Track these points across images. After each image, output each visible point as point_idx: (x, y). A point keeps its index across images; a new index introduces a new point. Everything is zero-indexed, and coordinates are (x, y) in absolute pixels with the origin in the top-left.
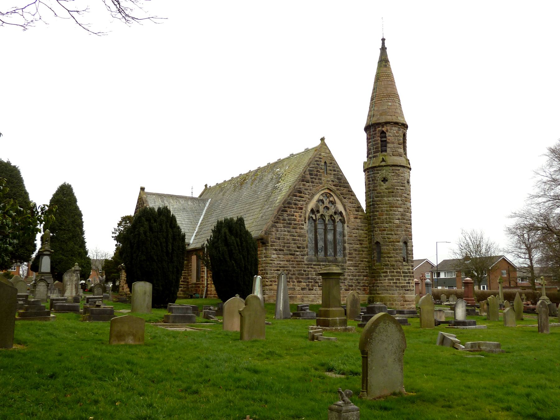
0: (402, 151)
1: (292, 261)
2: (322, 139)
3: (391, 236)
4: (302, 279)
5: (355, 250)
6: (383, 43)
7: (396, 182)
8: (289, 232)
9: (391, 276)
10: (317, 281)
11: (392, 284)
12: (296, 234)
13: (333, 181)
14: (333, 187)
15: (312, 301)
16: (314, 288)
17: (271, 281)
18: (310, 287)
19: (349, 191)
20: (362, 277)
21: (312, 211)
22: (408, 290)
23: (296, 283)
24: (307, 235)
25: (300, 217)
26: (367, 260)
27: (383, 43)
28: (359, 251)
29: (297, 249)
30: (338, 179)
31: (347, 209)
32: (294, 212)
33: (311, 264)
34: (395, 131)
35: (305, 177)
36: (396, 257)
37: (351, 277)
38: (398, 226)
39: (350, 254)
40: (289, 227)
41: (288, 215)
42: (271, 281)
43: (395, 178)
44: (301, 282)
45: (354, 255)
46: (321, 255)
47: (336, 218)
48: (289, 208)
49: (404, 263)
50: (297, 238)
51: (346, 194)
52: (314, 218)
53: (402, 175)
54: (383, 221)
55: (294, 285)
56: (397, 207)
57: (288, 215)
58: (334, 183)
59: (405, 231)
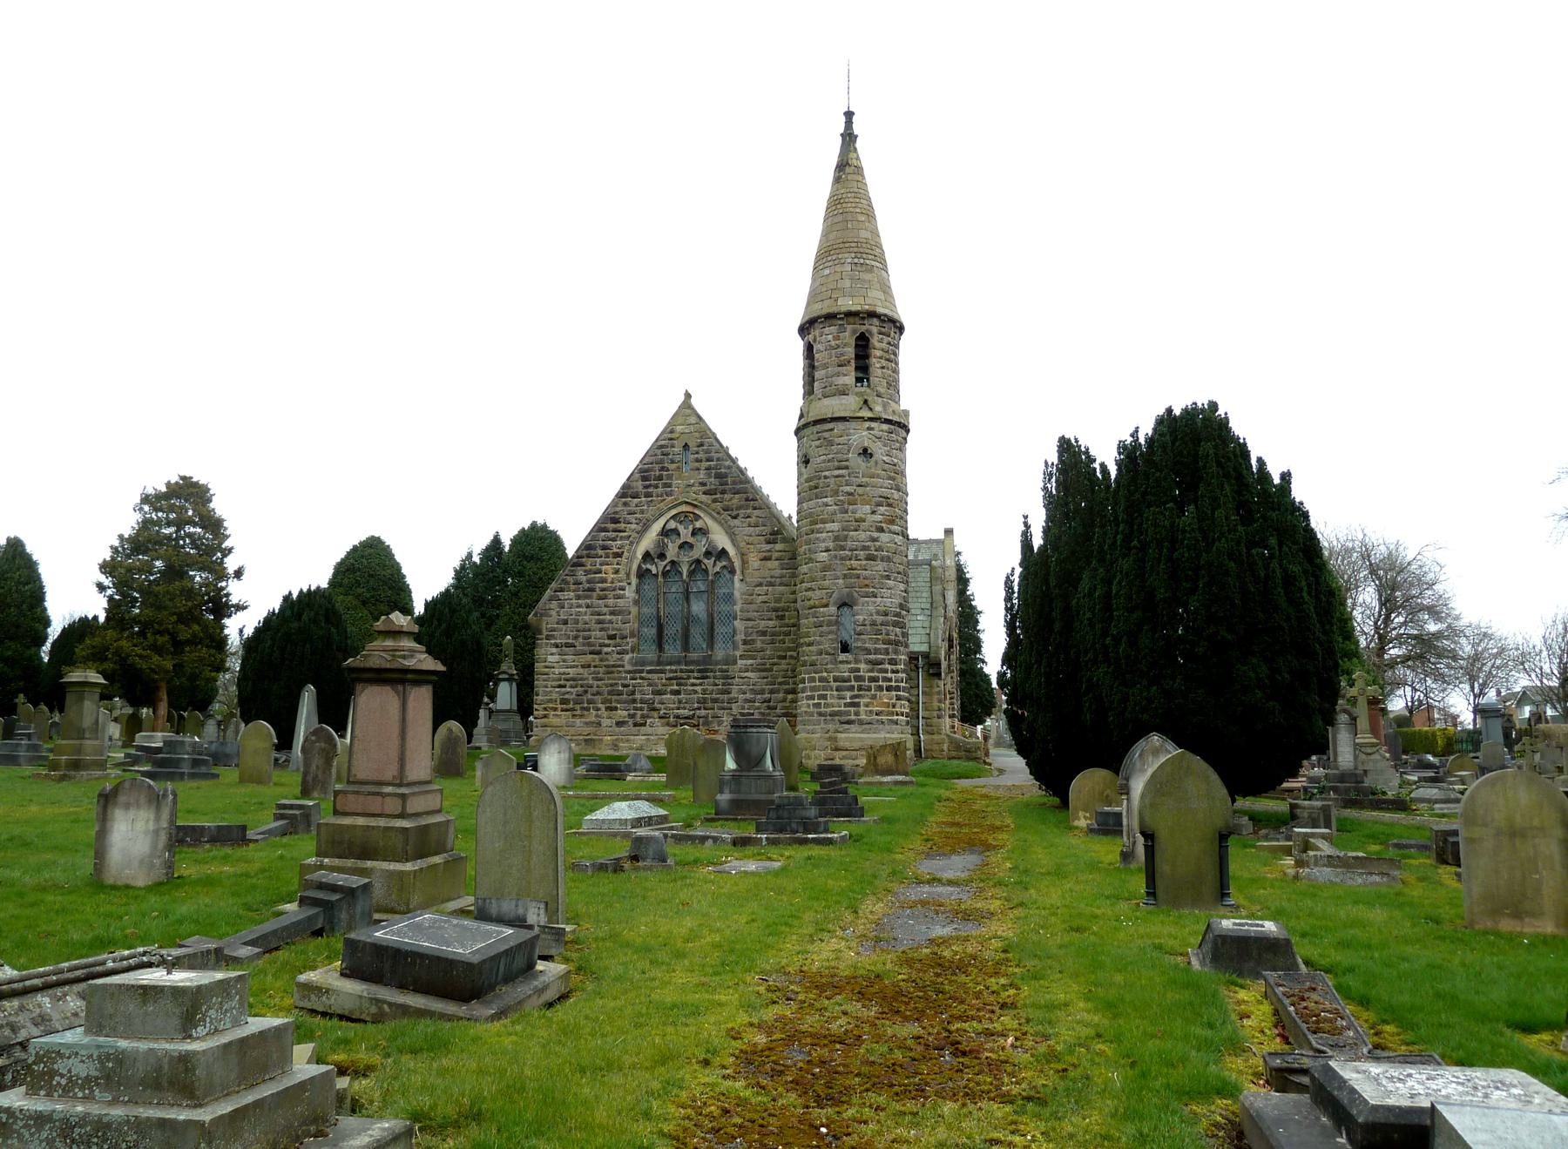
0: (849, 378)
2: (688, 396)
5: (764, 633)
14: (704, 498)
18: (638, 719)
20: (781, 695)
21: (647, 556)
22: (849, 722)
23: (603, 713)
28: (773, 634)
30: (718, 476)
36: (819, 643)
37: (748, 696)
39: (745, 642)
40: (587, 597)
41: (587, 572)
43: (822, 451)
45: (759, 645)
46: (673, 650)
47: (709, 569)
48: (588, 556)
49: (842, 657)
51: (739, 508)
56: (824, 522)
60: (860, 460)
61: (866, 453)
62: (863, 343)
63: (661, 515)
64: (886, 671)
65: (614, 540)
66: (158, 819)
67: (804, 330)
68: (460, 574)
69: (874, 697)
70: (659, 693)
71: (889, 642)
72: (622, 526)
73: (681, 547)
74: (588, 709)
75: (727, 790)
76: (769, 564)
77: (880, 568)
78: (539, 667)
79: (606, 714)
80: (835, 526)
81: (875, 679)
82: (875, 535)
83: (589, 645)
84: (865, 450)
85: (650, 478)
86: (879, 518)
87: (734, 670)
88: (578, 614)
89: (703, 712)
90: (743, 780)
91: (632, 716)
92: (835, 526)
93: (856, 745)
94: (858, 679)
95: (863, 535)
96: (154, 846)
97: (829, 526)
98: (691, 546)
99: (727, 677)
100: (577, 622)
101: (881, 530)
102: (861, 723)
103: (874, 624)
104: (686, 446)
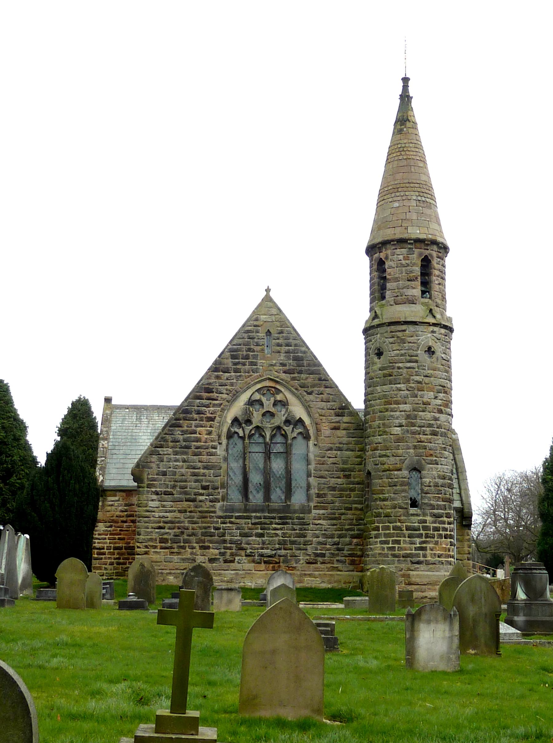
0: (417, 292)
1: (190, 512)
2: (268, 290)
3: (384, 459)
5: (333, 489)
6: (405, 87)
7: (397, 355)
8: (184, 461)
9: (386, 535)
11: (386, 551)
13: (283, 365)
14: (283, 376)
15: (230, 581)
16: (237, 558)
17: (146, 547)
18: (228, 557)
19: (320, 379)
20: (348, 539)
21: (236, 421)
22: (419, 563)
23: (198, 551)
24: (224, 466)
25: (210, 433)
26: (359, 506)
27: (405, 87)
29: (201, 491)
30: (296, 359)
32: (196, 427)
33: (231, 517)
34: (401, 257)
35: (220, 363)
36: (393, 499)
37: (321, 539)
39: (318, 496)
40: (186, 453)
42: (146, 547)
43: (395, 347)
44: (208, 548)
45: (329, 498)
48: (185, 419)
49: (412, 510)
50: (202, 471)
51: (313, 386)
52: (241, 434)
53: (410, 339)
54: (375, 432)
55: (192, 553)
56: (397, 403)
57: (184, 432)
58: (287, 368)
59: (415, 447)
60: (426, 356)
61: (430, 351)
62: (426, 263)
63: (248, 388)
64: (444, 523)
65: (207, 406)
66: (451, 630)
68: (22, 422)
69: (436, 543)
72: (215, 395)
73: (264, 415)
74: (184, 548)
75: (521, 614)
77: (440, 442)
79: (199, 552)
80: (407, 407)
81: (436, 529)
82: (437, 415)
83: (186, 493)
84: (430, 348)
85: (238, 357)
86: (439, 402)
87: (309, 518)
88: (175, 467)
89: (283, 552)
90: (533, 607)
92: (407, 407)
93: (425, 581)
94: (426, 528)
95: (428, 415)
96: (450, 647)
97: (402, 407)
98: (272, 415)
99: (304, 524)
100: (174, 474)
101: (440, 411)
102: (428, 563)
103: (436, 485)
104: (269, 333)
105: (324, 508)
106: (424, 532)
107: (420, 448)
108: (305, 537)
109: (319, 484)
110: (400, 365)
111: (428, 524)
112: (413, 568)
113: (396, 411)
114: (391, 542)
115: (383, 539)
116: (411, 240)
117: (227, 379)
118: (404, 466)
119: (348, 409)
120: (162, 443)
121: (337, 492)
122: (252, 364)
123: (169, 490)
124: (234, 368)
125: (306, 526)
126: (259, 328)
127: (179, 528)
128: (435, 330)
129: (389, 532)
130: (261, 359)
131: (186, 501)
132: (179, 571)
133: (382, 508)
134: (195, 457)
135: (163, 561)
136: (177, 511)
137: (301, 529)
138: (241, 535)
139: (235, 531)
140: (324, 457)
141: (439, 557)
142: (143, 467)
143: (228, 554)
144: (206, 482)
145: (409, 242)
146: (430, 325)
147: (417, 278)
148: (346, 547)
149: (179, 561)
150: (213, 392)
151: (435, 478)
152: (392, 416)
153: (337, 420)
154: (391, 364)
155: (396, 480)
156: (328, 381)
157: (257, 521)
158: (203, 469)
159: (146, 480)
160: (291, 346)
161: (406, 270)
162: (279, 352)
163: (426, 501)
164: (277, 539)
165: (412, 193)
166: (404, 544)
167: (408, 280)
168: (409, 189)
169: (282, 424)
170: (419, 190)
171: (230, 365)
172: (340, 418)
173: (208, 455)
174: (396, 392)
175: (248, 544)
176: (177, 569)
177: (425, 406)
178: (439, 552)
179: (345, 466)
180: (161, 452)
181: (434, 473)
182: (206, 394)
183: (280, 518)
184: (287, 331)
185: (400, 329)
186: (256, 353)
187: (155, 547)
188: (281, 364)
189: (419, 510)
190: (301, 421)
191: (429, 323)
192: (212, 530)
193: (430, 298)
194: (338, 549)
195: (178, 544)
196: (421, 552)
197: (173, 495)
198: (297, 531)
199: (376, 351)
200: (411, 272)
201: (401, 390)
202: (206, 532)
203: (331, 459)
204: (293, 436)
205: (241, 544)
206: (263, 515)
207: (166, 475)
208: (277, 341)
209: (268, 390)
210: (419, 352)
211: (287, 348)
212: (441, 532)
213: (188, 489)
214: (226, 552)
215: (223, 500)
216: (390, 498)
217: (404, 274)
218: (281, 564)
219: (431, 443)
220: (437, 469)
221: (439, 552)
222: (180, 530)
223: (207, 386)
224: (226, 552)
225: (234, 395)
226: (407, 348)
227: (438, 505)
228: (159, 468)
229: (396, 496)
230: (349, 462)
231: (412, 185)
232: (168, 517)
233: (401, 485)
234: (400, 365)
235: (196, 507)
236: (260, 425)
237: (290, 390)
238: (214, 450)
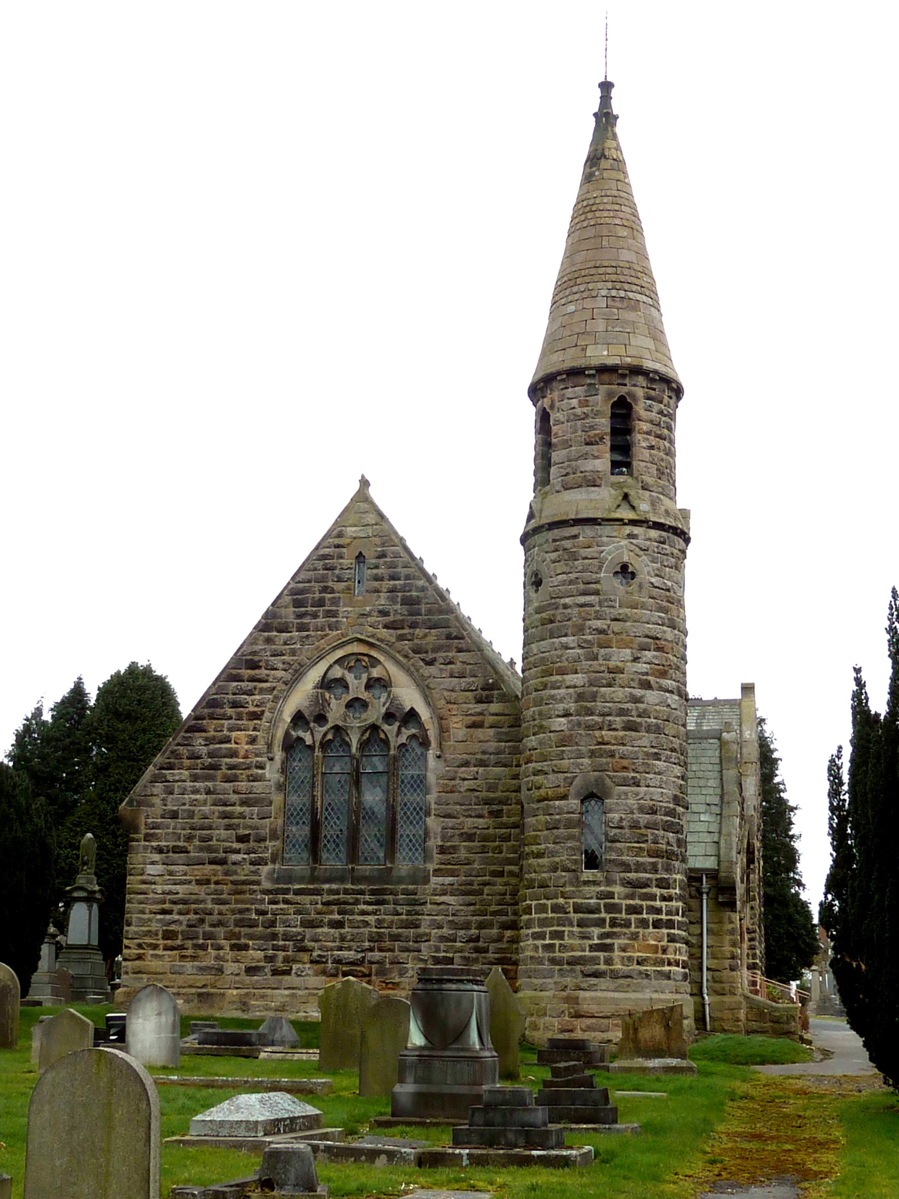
0: (602, 463)
1: (217, 883)
2: (365, 483)
3: (539, 779)
4: (251, 937)
5: (470, 837)
7: (563, 583)
8: (209, 792)
10: (308, 944)
11: (541, 953)
12: (234, 798)
13: (384, 613)
14: (384, 633)
16: (295, 967)
18: (279, 964)
19: (449, 637)
20: (495, 931)
21: (299, 718)
22: (596, 975)
28: (485, 839)
29: (236, 845)
30: (406, 601)
31: (436, 694)
32: (230, 730)
34: (575, 402)
36: (553, 854)
37: (446, 931)
38: (564, 741)
39: (442, 850)
40: (212, 778)
41: (209, 741)
42: (140, 946)
43: (560, 567)
44: (246, 947)
45: (463, 854)
46: (333, 860)
49: (588, 875)
50: (238, 809)
51: (436, 649)
52: (309, 741)
55: (217, 958)
56: (562, 672)
57: (209, 741)
59: (592, 754)
61: (625, 571)
63: (321, 658)
64: (653, 897)
67: (536, 391)
68: (23, 738)
69: (634, 937)
70: (312, 924)
71: (656, 854)
72: (263, 672)
73: (349, 705)
74: (203, 947)
76: (479, 733)
77: (645, 742)
78: (132, 882)
80: (578, 679)
82: (638, 692)
83: (210, 850)
84: (624, 567)
86: (642, 667)
87: (425, 891)
88: (193, 803)
89: (377, 955)
91: (270, 959)
92: (578, 679)
93: (608, 1010)
95: (619, 693)
97: (570, 679)
98: (365, 705)
99: (415, 903)
101: (647, 685)
102: (615, 975)
103: (635, 826)
104: (360, 557)
105: (452, 874)
106: (608, 917)
107: (601, 756)
108: (417, 926)
109: (444, 828)
110: (567, 600)
111: (616, 901)
112: (584, 985)
113: (559, 688)
114: (547, 936)
115: (537, 930)
116: (591, 369)
117: (285, 644)
118: (572, 790)
119: (500, 689)
120: (172, 760)
121: (476, 844)
122: (330, 614)
123: (181, 844)
124: (298, 623)
125: (418, 908)
126: (344, 550)
127: (196, 913)
128: (636, 532)
129: (544, 915)
130: (345, 606)
131: (210, 863)
132: (193, 990)
133: (535, 872)
134: (227, 785)
135: (168, 971)
136: (194, 883)
137: (409, 913)
138: (304, 924)
139: (293, 916)
140: (454, 779)
141: (638, 963)
142: (140, 804)
143: (280, 959)
144: (245, 828)
145: (587, 372)
146: (625, 524)
147: (602, 438)
148: (492, 947)
149: (195, 971)
150: (260, 667)
151: (632, 813)
152: (552, 697)
153: (477, 710)
154: (553, 601)
155: (557, 817)
156: (463, 638)
157: (332, 897)
158: (240, 805)
159: (143, 827)
160: (399, 579)
161: (583, 425)
162: (377, 591)
163: (613, 856)
164: (366, 930)
165: (600, 285)
166: (570, 938)
167: (587, 444)
168: (596, 278)
169: (380, 720)
170: (614, 277)
171: (291, 619)
172: (486, 705)
173: (249, 781)
174: (559, 652)
175: (316, 941)
176: (191, 986)
177: (613, 675)
178: (640, 954)
179: (492, 795)
180: (170, 778)
181: (631, 801)
182: (249, 671)
183: (373, 892)
184: (393, 553)
185: (568, 535)
186: (337, 595)
187: (155, 947)
188: (380, 612)
189: (599, 874)
190: (412, 716)
191: (621, 520)
192: (254, 916)
193: (630, 474)
194: (477, 950)
195: (195, 942)
196: (601, 955)
197: (188, 852)
198: (404, 917)
199: (533, 579)
200: (592, 428)
201: (567, 648)
202: (241, 920)
203: (466, 782)
204: (399, 743)
205: (302, 940)
206: (342, 886)
207: (177, 818)
208: (375, 571)
209: (358, 660)
210: (602, 575)
211: (392, 582)
212: (645, 916)
213: (214, 842)
214: (275, 956)
215: (274, 861)
216: (551, 853)
217: (579, 433)
218: (373, 978)
219: (624, 745)
220: (637, 794)
221: (640, 954)
222: (198, 916)
223: (250, 657)
224: (275, 956)
225: (296, 671)
226: (580, 568)
227: (638, 864)
228: (165, 805)
229: (558, 847)
230: (500, 788)
231: (601, 271)
232: (177, 893)
233: (567, 827)
234: (567, 600)
235: (226, 874)
236: (340, 724)
237: (393, 658)
238: (260, 771)
